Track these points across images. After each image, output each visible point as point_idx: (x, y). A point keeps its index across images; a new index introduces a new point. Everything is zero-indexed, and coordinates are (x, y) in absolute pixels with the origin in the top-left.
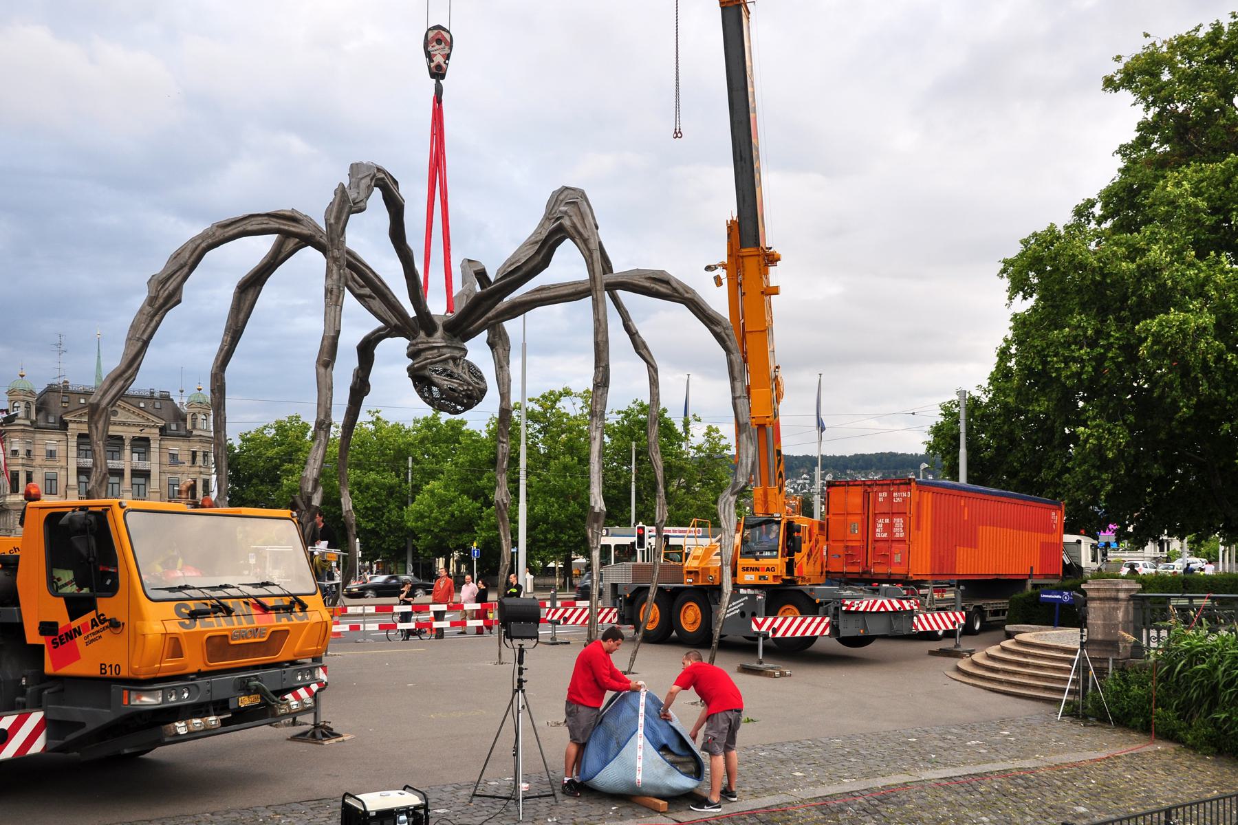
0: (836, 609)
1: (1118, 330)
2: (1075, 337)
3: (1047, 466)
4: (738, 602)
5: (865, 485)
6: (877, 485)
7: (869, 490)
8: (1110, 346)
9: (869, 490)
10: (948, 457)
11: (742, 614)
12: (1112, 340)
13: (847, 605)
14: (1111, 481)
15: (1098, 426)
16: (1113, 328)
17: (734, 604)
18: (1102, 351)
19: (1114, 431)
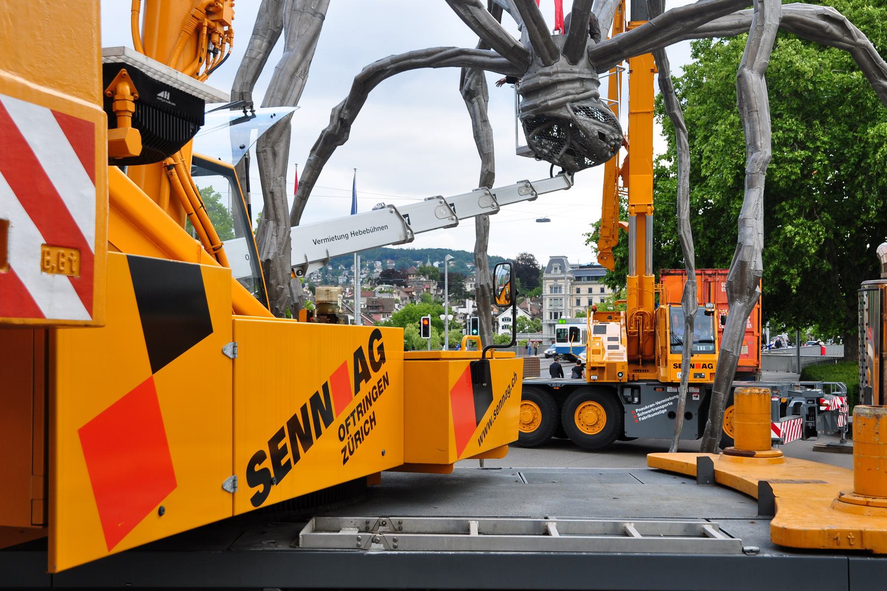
0: (811, 409)
1: (824, 134)
2: (786, 140)
3: (719, 259)
4: (664, 401)
5: (705, 274)
6: (719, 274)
7: (710, 279)
8: (817, 149)
9: (710, 279)
10: (621, 249)
11: (672, 415)
12: (819, 144)
13: (827, 405)
14: (798, 275)
15: (802, 224)
16: (821, 133)
17: (657, 403)
18: (810, 154)
19: (814, 228)
